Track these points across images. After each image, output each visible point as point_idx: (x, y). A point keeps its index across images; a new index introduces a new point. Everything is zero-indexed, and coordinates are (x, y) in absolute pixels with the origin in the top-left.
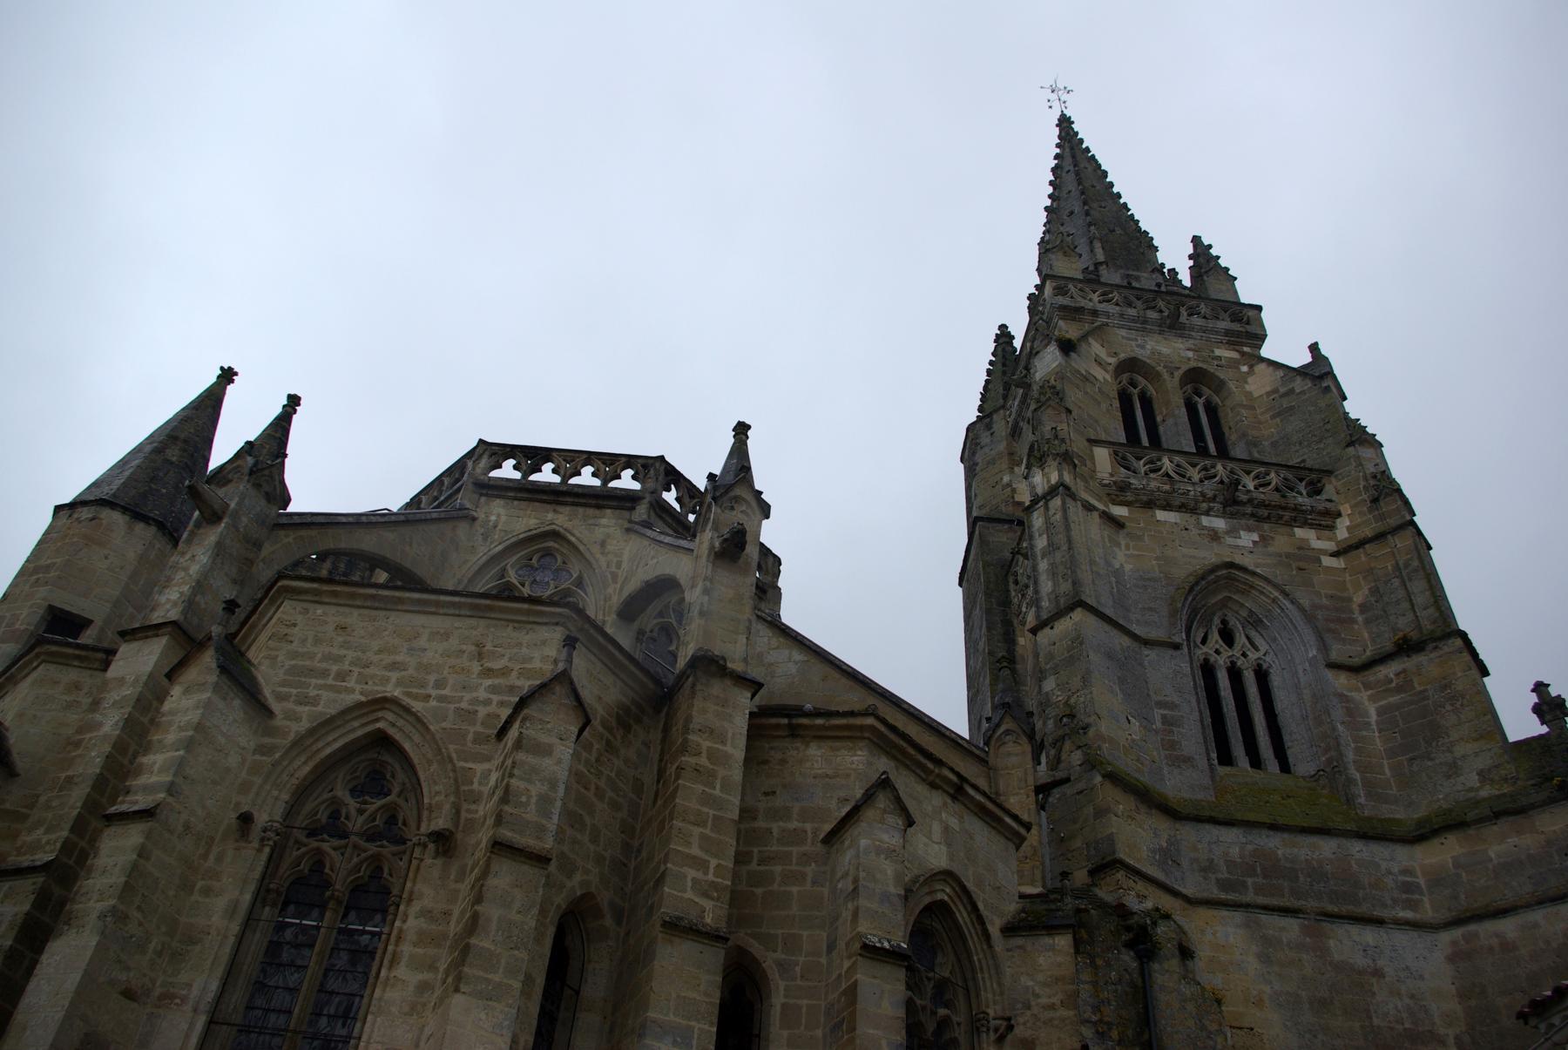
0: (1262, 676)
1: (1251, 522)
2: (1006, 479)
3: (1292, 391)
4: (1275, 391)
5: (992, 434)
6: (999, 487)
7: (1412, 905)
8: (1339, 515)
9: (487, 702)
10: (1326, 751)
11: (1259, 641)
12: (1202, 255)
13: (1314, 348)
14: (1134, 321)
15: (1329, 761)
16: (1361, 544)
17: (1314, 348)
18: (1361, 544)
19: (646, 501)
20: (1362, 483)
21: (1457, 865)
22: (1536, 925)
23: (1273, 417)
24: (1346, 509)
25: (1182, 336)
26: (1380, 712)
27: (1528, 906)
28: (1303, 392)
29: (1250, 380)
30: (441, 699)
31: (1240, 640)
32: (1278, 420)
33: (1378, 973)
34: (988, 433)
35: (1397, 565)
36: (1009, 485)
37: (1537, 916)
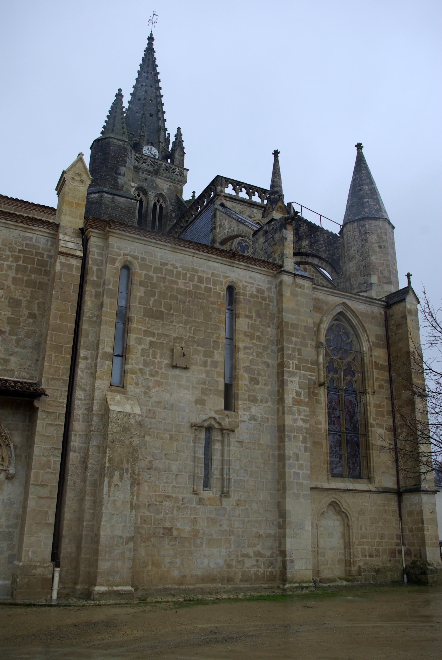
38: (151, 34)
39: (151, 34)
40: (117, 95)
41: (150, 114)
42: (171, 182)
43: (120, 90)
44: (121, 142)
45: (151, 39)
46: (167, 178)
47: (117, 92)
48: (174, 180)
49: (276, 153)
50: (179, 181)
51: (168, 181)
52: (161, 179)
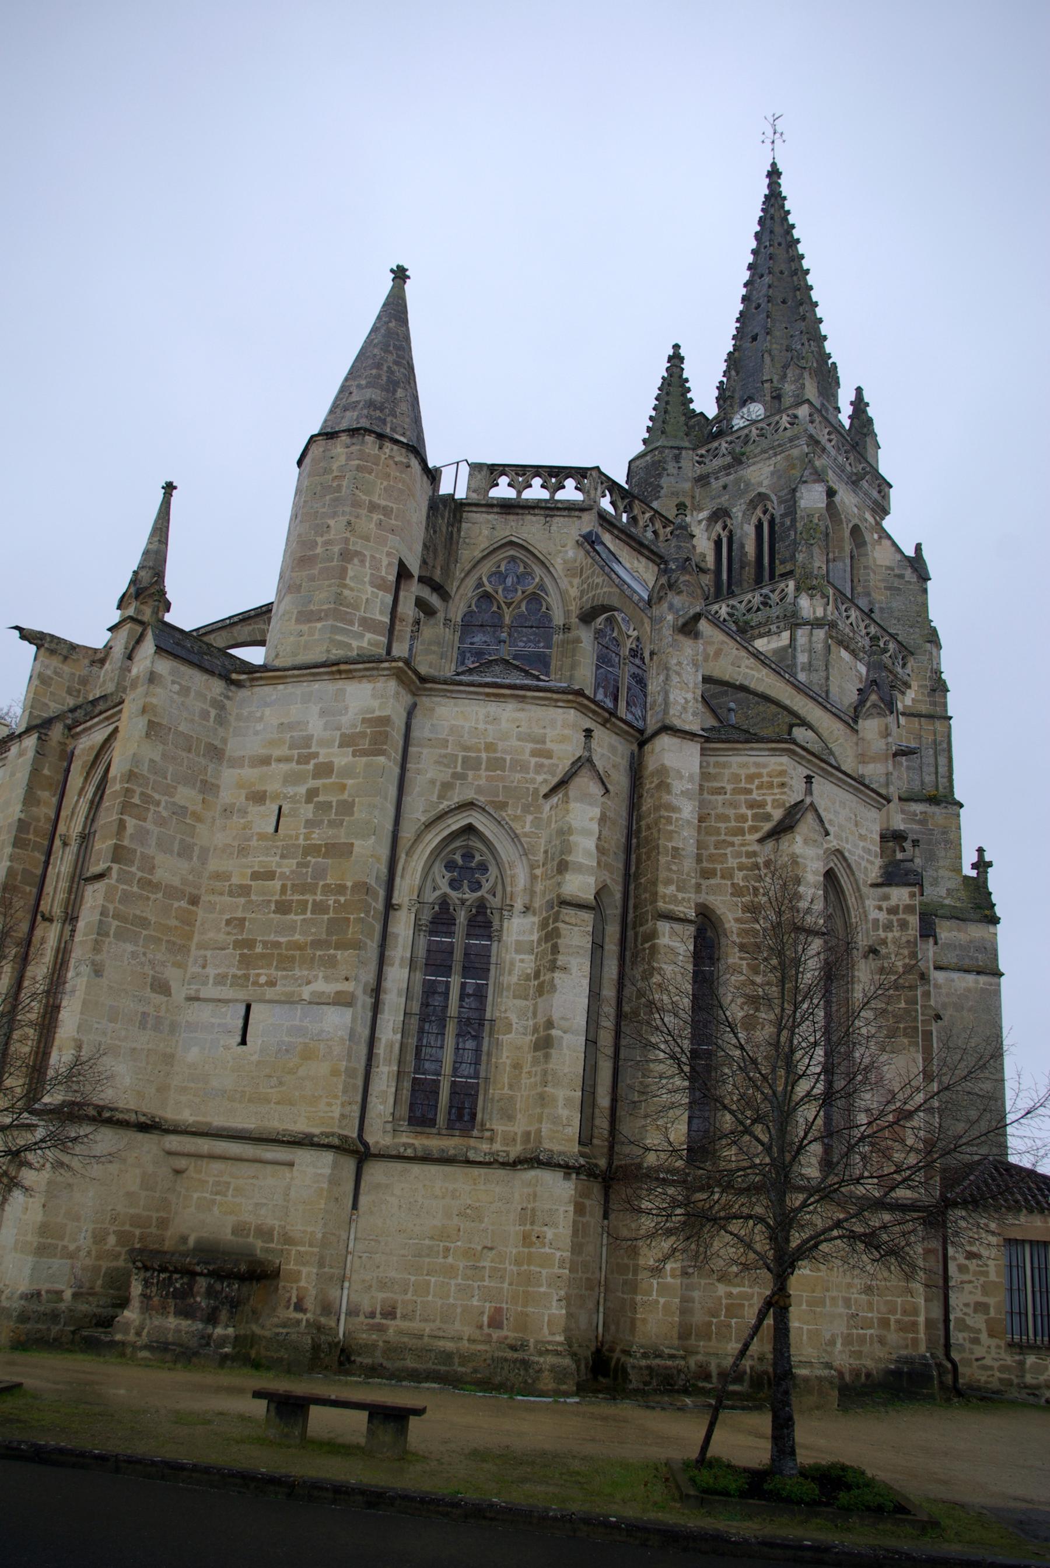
3: (901, 576)
4: (891, 569)
5: (680, 468)
8: (909, 687)
12: (859, 404)
13: (918, 548)
14: (838, 467)
16: (919, 716)
17: (918, 548)
18: (919, 716)
20: (929, 674)
22: (953, 980)
23: (886, 588)
24: (914, 685)
25: (854, 492)
27: (953, 970)
32: (888, 592)
34: (676, 465)
35: (935, 740)
37: (955, 975)
38: (774, 165)
39: (774, 165)
40: (670, 359)
41: (757, 335)
42: (775, 455)
43: (676, 347)
44: (648, 458)
45: (774, 174)
46: (764, 451)
47: (671, 352)
48: (780, 445)
49: (169, 488)
50: (791, 440)
51: (770, 458)
52: (754, 464)
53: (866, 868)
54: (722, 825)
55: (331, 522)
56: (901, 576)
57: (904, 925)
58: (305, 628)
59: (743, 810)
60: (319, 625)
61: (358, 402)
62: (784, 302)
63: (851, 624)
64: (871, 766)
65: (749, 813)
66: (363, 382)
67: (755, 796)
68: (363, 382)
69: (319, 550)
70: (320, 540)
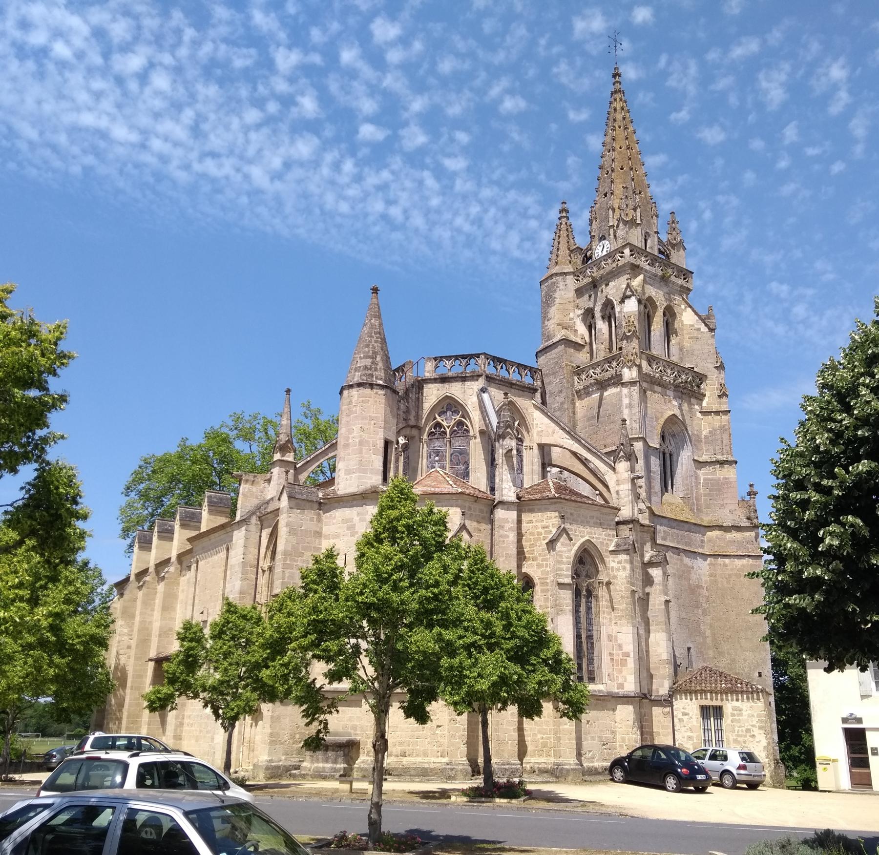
0: (671, 455)
1: (680, 394)
2: (572, 315)
3: (699, 329)
4: (693, 326)
6: (568, 317)
7: (702, 547)
9: (605, 539)
10: (686, 490)
11: (672, 442)
15: (687, 494)
19: (539, 391)
21: (717, 538)
24: (708, 393)
26: (705, 479)
28: (703, 332)
29: (684, 314)
30: (597, 538)
31: (667, 441)
33: (693, 568)
34: (563, 283)
36: (572, 319)
41: (607, 193)
53: (607, 544)
54: (532, 537)
55: (354, 428)
56: (699, 329)
57: (624, 568)
58: (348, 477)
59: (541, 530)
60: (353, 475)
61: (360, 367)
62: (622, 169)
63: (661, 371)
64: (622, 486)
65: (543, 531)
66: (362, 356)
67: (545, 523)
68: (362, 356)
69: (351, 441)
70: (351, 436)
